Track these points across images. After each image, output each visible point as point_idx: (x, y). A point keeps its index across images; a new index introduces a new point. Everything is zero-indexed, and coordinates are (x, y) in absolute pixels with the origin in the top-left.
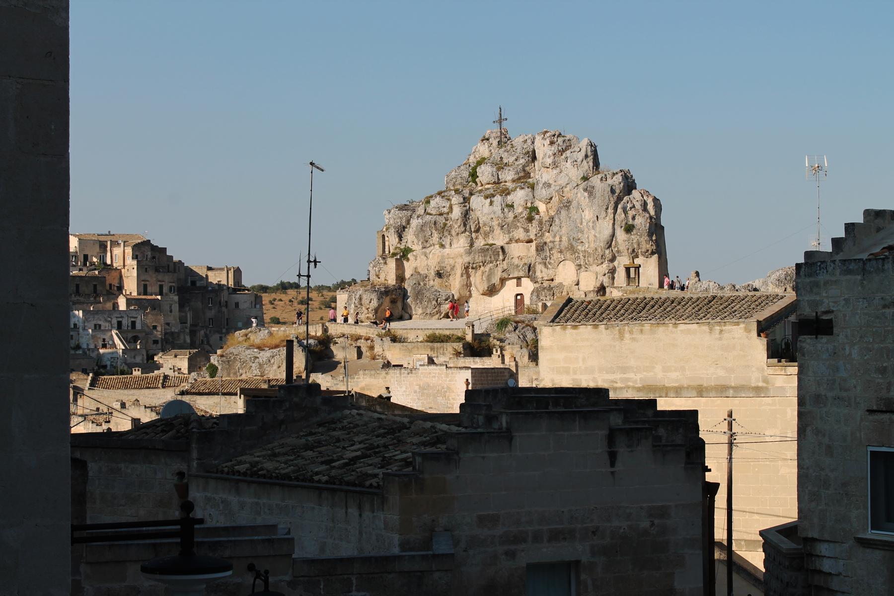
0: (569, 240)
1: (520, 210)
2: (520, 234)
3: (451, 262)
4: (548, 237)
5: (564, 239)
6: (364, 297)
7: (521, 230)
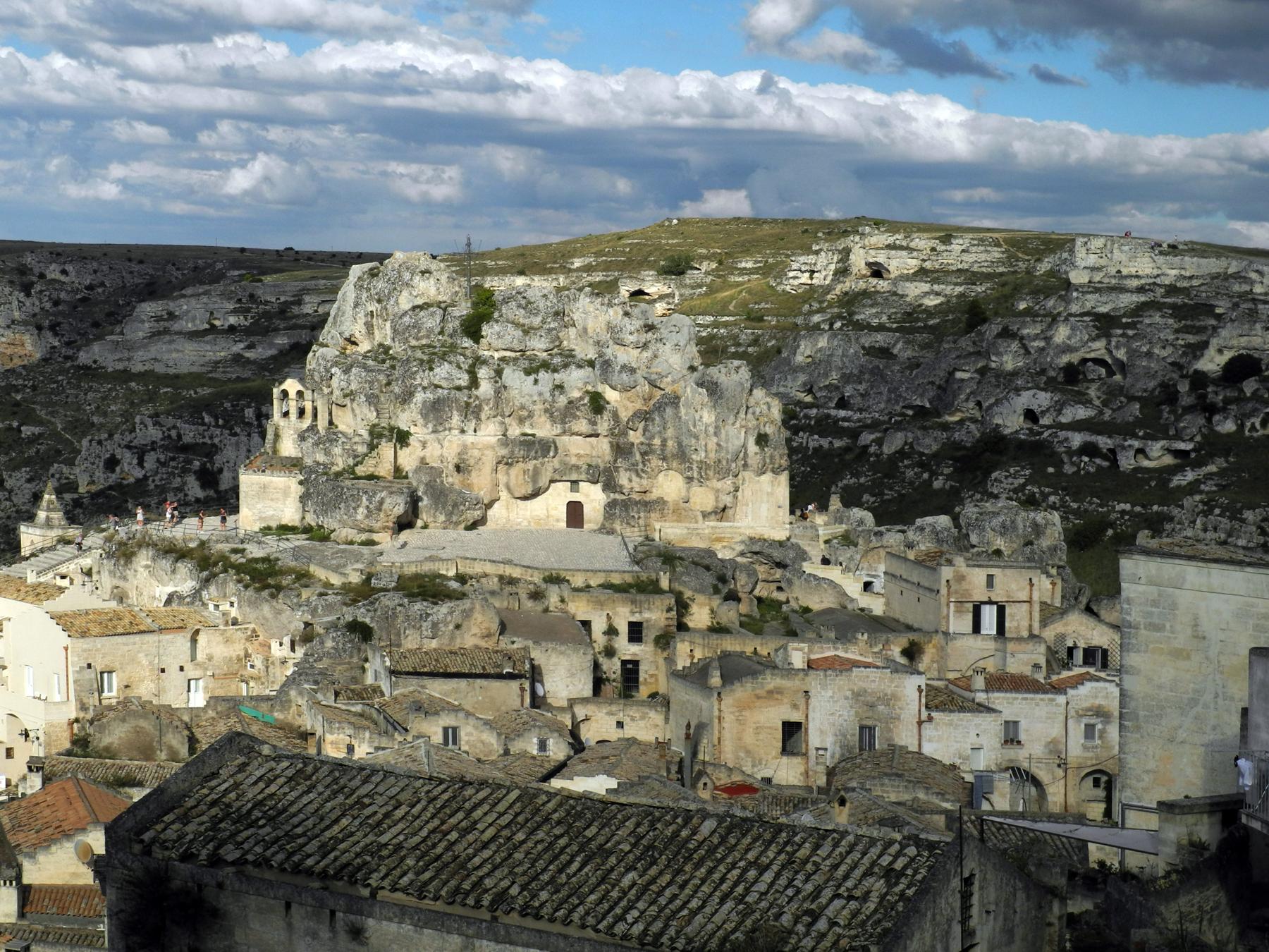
0: (680, 445)
1: (576, 394)
2: (582, 425)
3: (476, 453)
4: (635, 437)
5: (670, 443)
6: (388, 500)
7: (584, 422)
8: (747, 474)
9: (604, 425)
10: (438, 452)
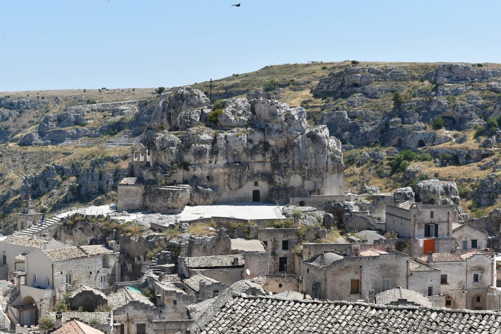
0: (300, 163)
5: (296, 162)
7: (260, 155)
8: (328, 174)
9: (268, 155)
10: (200, 173)
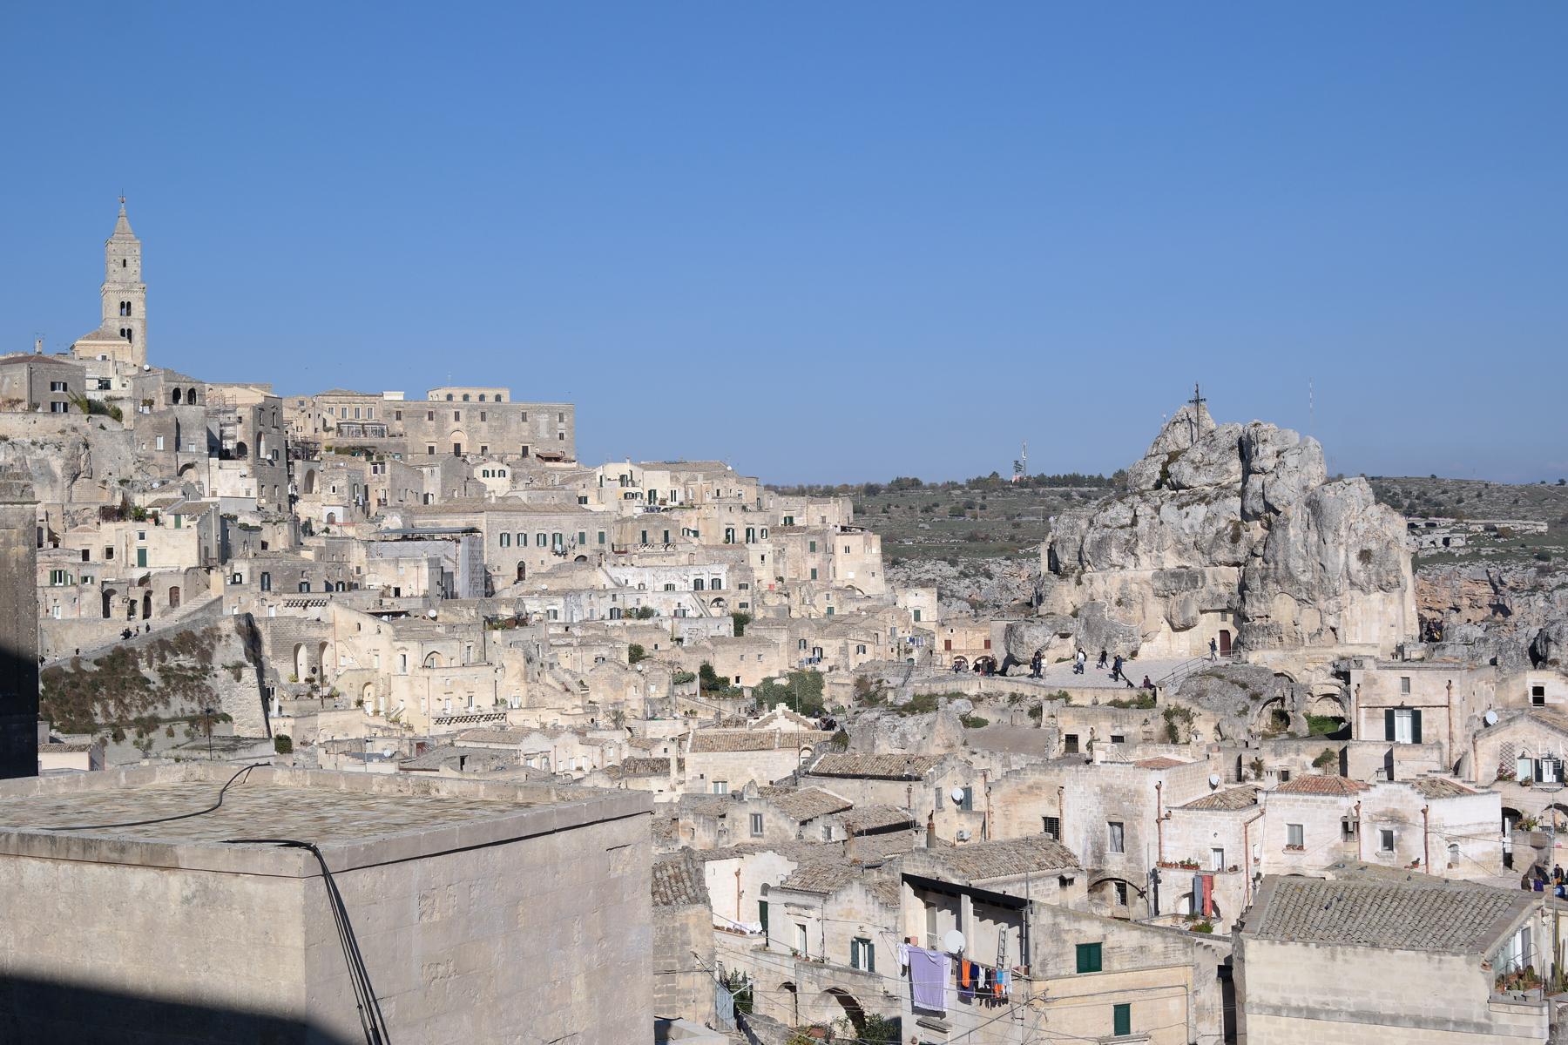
9: (1242, 553)
10: (1101, 590)
